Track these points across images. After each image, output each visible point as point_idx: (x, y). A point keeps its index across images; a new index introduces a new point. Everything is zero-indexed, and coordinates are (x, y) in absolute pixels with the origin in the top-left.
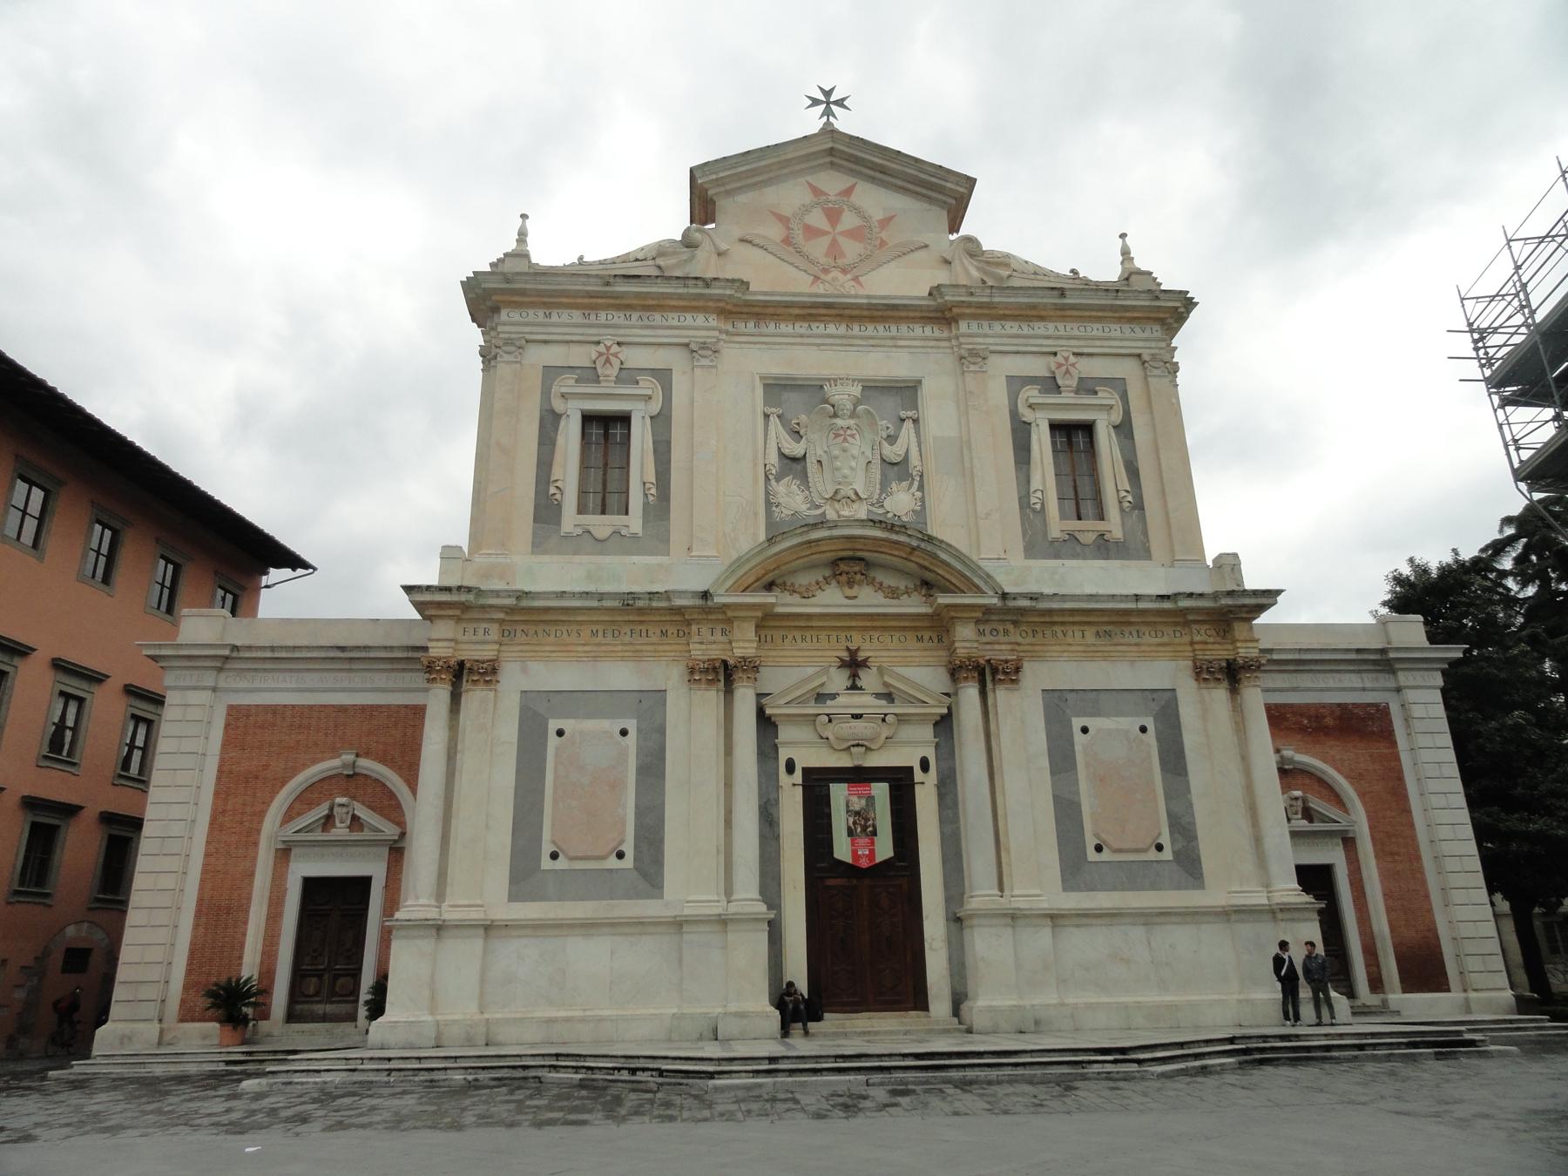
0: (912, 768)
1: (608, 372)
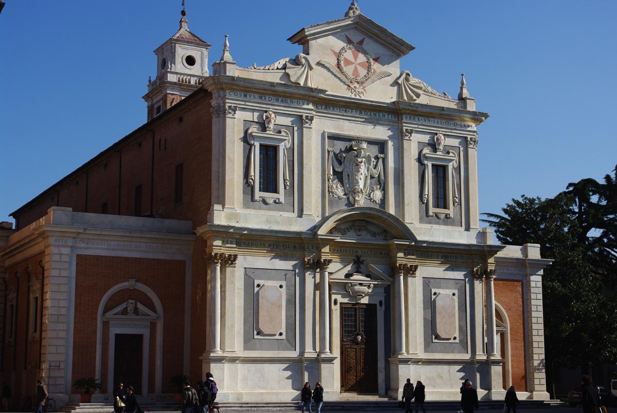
0: (376, 304)
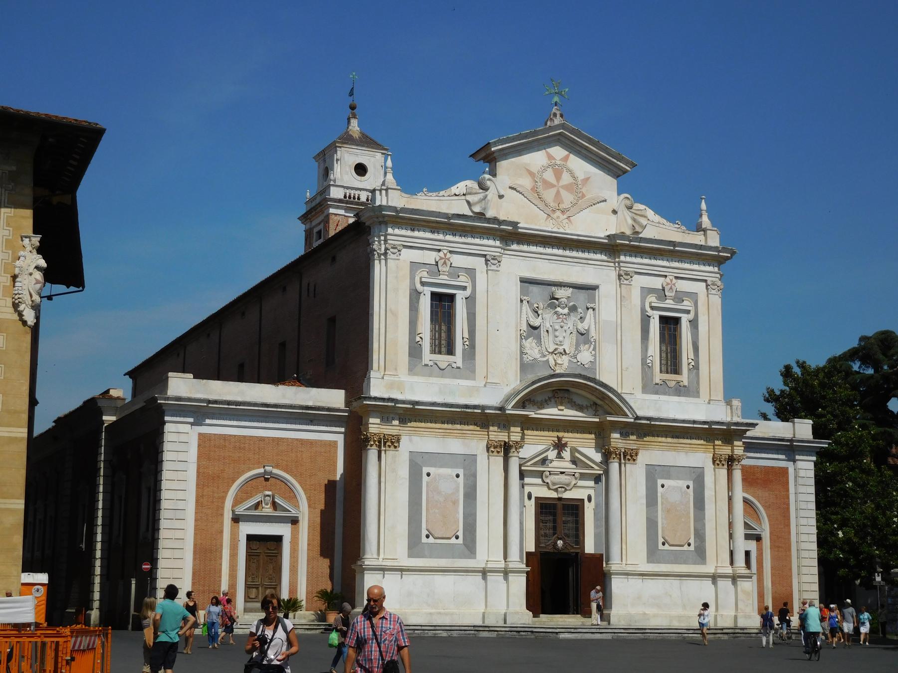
0: (584, 500)
1: (444, 269)
